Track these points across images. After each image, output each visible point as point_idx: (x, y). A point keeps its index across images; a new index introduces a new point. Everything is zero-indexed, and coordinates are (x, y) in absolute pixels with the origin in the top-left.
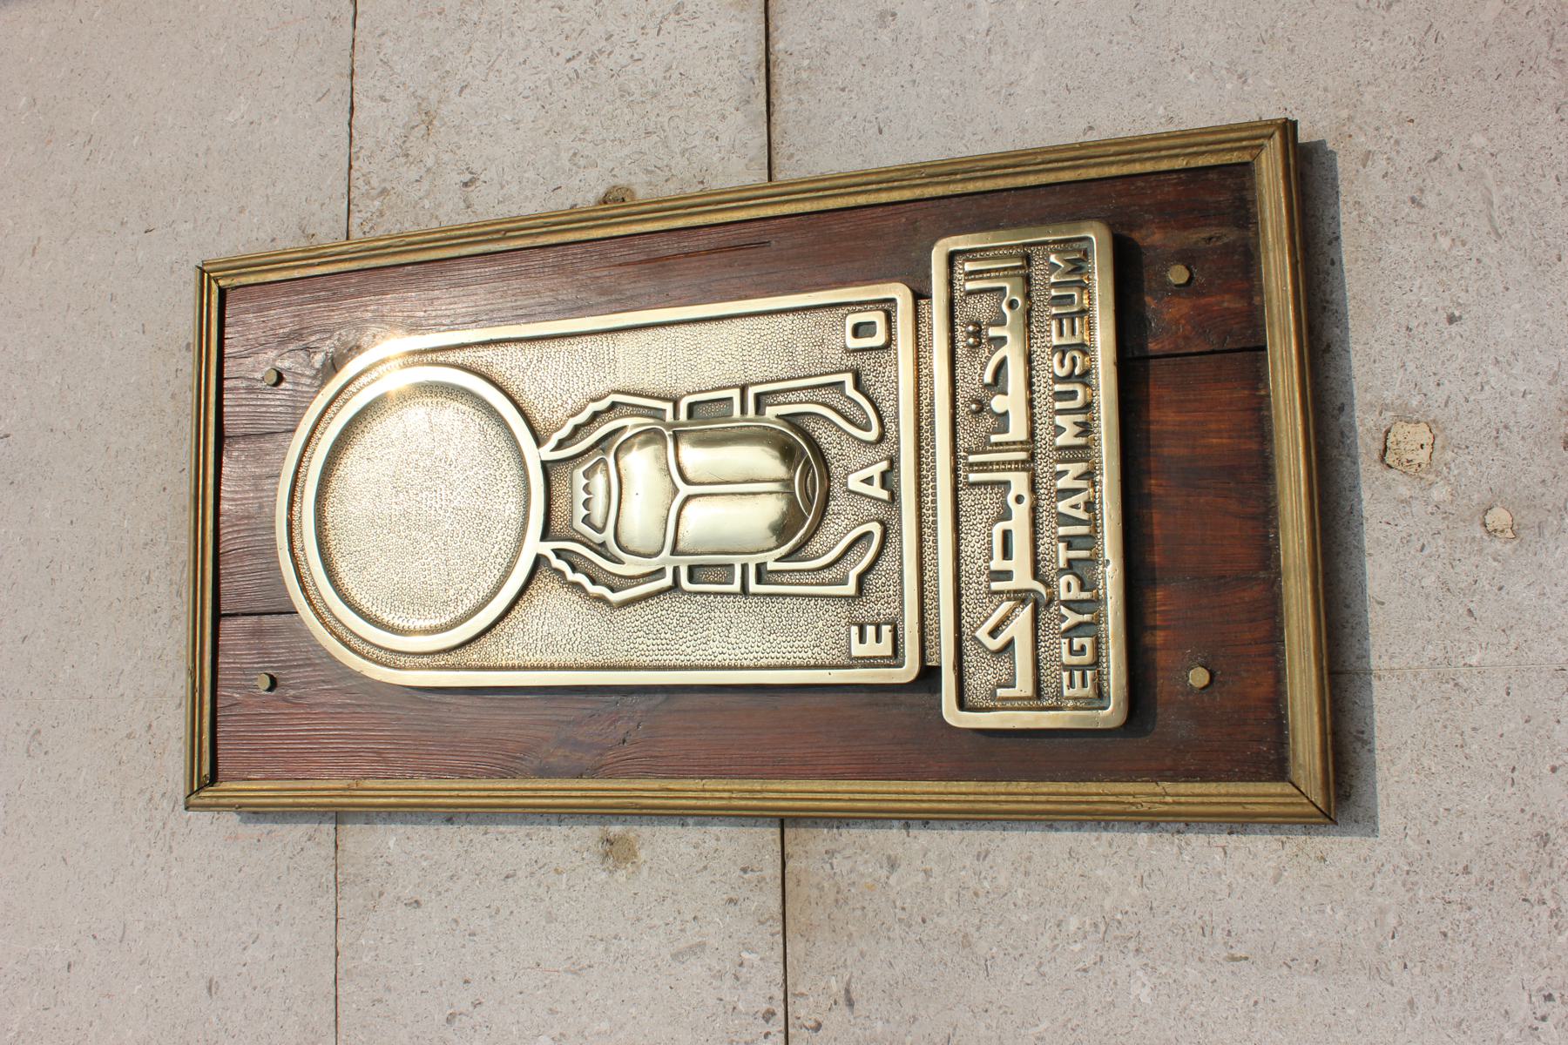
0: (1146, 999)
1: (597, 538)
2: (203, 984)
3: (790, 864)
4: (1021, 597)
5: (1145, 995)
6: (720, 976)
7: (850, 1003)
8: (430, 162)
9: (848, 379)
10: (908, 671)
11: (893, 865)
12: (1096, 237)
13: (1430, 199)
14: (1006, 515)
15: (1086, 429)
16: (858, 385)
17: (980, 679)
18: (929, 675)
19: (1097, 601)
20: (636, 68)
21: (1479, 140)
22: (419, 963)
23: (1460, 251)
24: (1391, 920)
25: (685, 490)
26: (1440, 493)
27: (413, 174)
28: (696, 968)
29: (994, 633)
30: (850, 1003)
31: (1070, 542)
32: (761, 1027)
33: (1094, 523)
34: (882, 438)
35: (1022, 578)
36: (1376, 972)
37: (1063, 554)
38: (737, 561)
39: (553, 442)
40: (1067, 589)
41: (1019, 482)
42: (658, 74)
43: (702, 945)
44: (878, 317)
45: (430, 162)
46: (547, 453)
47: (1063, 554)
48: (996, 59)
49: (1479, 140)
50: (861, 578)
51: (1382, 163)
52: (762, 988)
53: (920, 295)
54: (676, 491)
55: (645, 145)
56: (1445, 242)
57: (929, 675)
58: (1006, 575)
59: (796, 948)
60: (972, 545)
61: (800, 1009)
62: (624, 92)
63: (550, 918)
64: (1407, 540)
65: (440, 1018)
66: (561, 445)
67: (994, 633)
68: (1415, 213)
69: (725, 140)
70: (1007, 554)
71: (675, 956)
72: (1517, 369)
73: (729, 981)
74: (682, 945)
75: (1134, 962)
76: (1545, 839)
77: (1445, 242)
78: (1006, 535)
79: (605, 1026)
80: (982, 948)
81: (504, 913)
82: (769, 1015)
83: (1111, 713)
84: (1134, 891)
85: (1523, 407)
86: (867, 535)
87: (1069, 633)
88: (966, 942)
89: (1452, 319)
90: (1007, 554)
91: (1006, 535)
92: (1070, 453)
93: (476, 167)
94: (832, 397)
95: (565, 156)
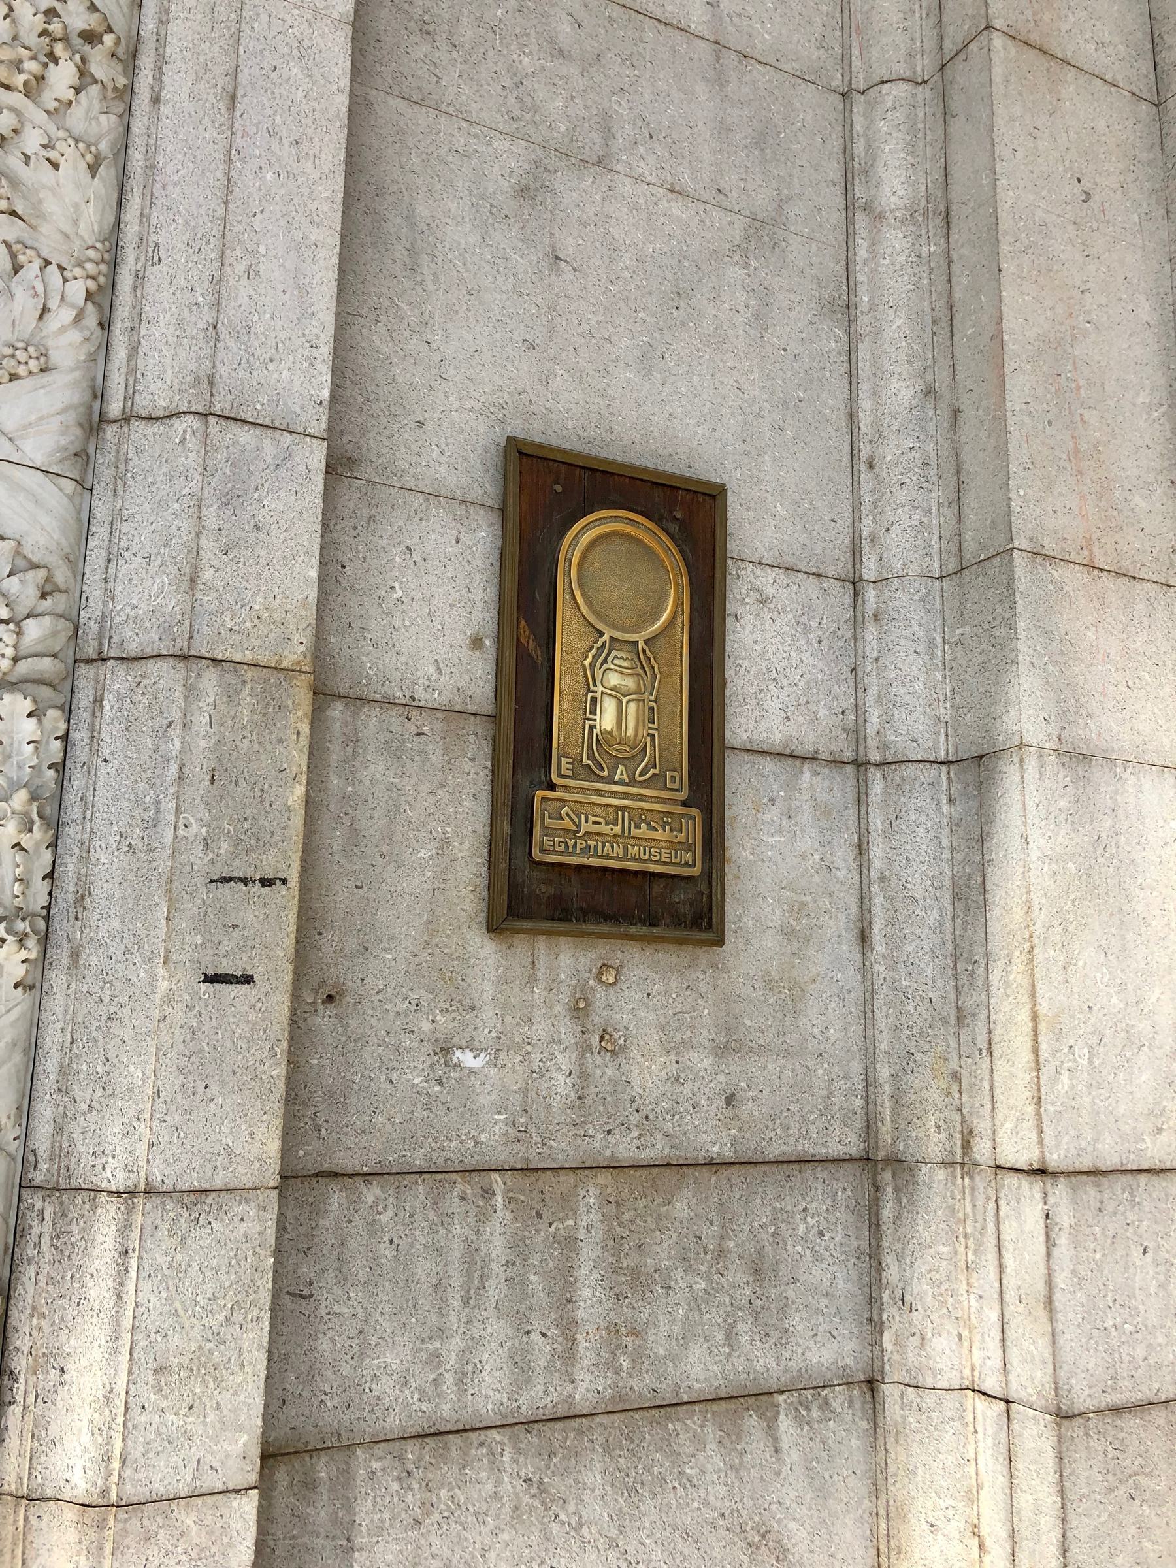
0: (421, 854)
1: (609, 660)
2: (422, 419)
3: (472, 718)
4: (579, 827)
5: (421, 854)
6: (429, 680)
7: (418, 734)
8: (747, 600)
9: (657, 771)
10: (555, 778)
11: (472, 760)
12: (696, 871)
13: (689, 992)
14: (607, 823)
15: (633, 859)
16: (654, 774)
17: (552, 806)
18: (552, 787)
19: (578, 855)
20: (769, 698)
21: (706, 1012)
22: (433, 537)
23: (670, 1001)
24: (446, 951)
25: (624, 700)
26: (591, 982)
27: (744, 592)
28: (432, 669)
29: (567, 814)
30: (418, 734)
31: (596, 847)
32: (408, 695)
33: (600, 857)
34: (636, 781)
35: (585, 828)
36: (427, 943)
37: (592, 843)
38: (597, 717)
39: (646, 648)
40: (581, 844)
41: (617, 830)
42: (765, 706)
43: (441, 673)
44: (676, 786)
45: (747, 600)
46: (641, 644)
47: (592, 843)
48: (753, 841)
49: (706, 1012)
50: (589, 766)
51: (702, 977)
52: (426, 697)
53: (684, 804)
54: (625, 696)
55: (740, 698)
56: (674, 996)
57: (552, 787)
58: (586, 822)
59: (440, 715)
60: (597, 810)
61: (414, 713)
62: (761, 691)
63: (452, 606)
64: (577, 970)
65: (409, 543)
66: (644, 651)
67: (567, 814)
68: (684, 986)
69: (738, 731)
70: (594, 823)
71: (436, 660)
72: (631, 1016)
73: (427, 683)
74: (441, 665)
75: (434, 851)
76: (473, 1009)
77: (674, 996)
78: (599, 823)
79: (407, 623)
80: (440, 792)
81: (454, 584)
82: (413, 698)
83: (537, 855)
84: (460, 855)
85: (618, 1016)
86: (602, 770)
87: (566, 844)
88: (442, 786)
89: (649, 995)
90: (594, 823)
91: (599, 823)
92: (625, 850)
93: (742, 621)
94: (651, 763)
95: (741, 662)
